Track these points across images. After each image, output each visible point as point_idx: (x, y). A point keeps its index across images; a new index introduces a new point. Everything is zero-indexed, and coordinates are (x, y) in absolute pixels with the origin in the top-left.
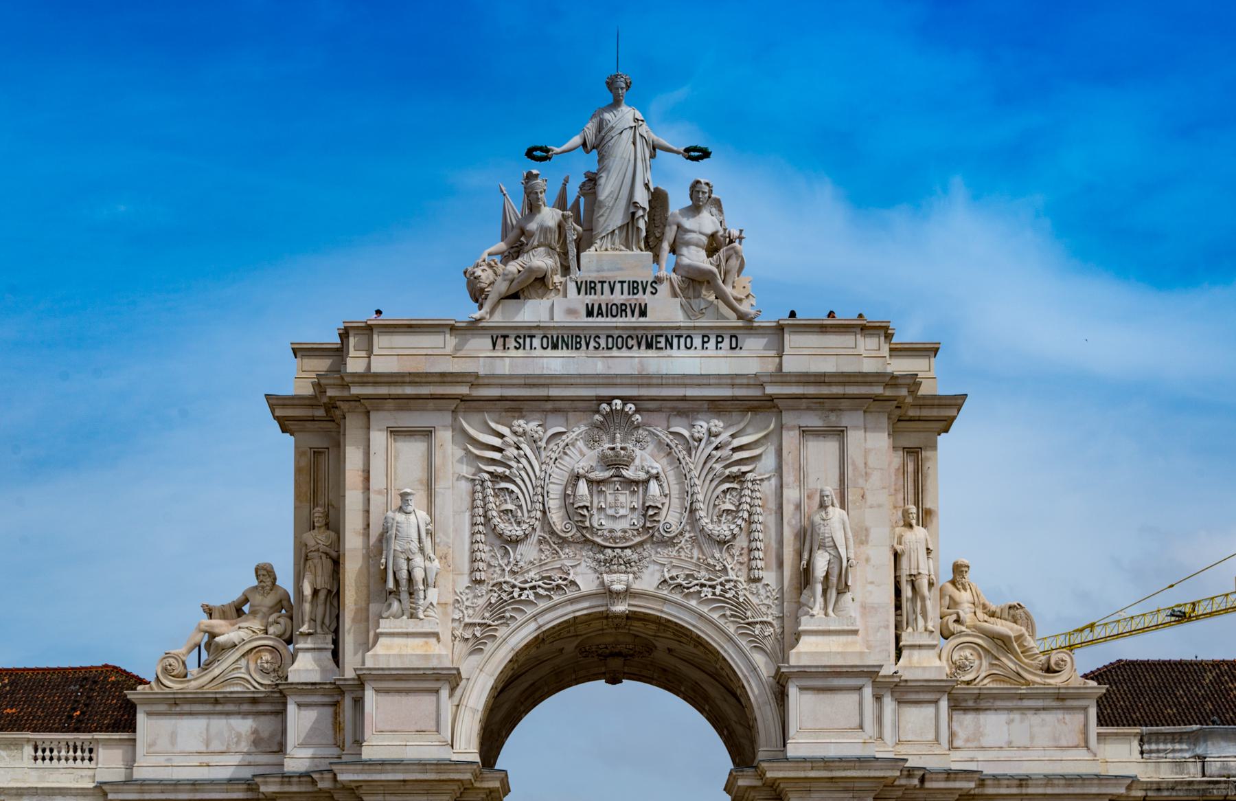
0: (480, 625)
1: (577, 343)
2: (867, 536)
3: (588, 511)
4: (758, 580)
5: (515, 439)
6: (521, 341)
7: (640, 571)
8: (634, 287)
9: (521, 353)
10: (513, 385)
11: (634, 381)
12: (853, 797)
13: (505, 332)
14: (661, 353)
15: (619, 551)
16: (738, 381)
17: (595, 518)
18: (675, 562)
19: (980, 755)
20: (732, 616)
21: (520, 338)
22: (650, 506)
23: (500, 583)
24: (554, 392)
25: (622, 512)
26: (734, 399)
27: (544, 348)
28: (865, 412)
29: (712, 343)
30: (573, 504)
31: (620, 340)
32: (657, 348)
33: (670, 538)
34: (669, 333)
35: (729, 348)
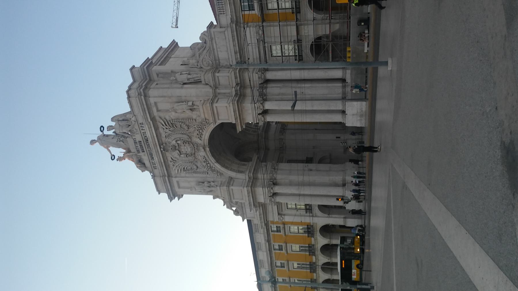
0: (217, 173)
4: (195, 120)
7: (199, 143)
8: (135, 143)
9: (156, 164)
10: (163, 169)
11: (156, 147)
12: (244, 108)
13: (153, 168)
14: (148, 138)
16: (150, 127)
18: (195, 137)
19: (231, 59)
20: (205, 126)
22: (183, 144)
24: (162, 161)
25: (186, 148)
26: (154, 126)
34: (143, 137)
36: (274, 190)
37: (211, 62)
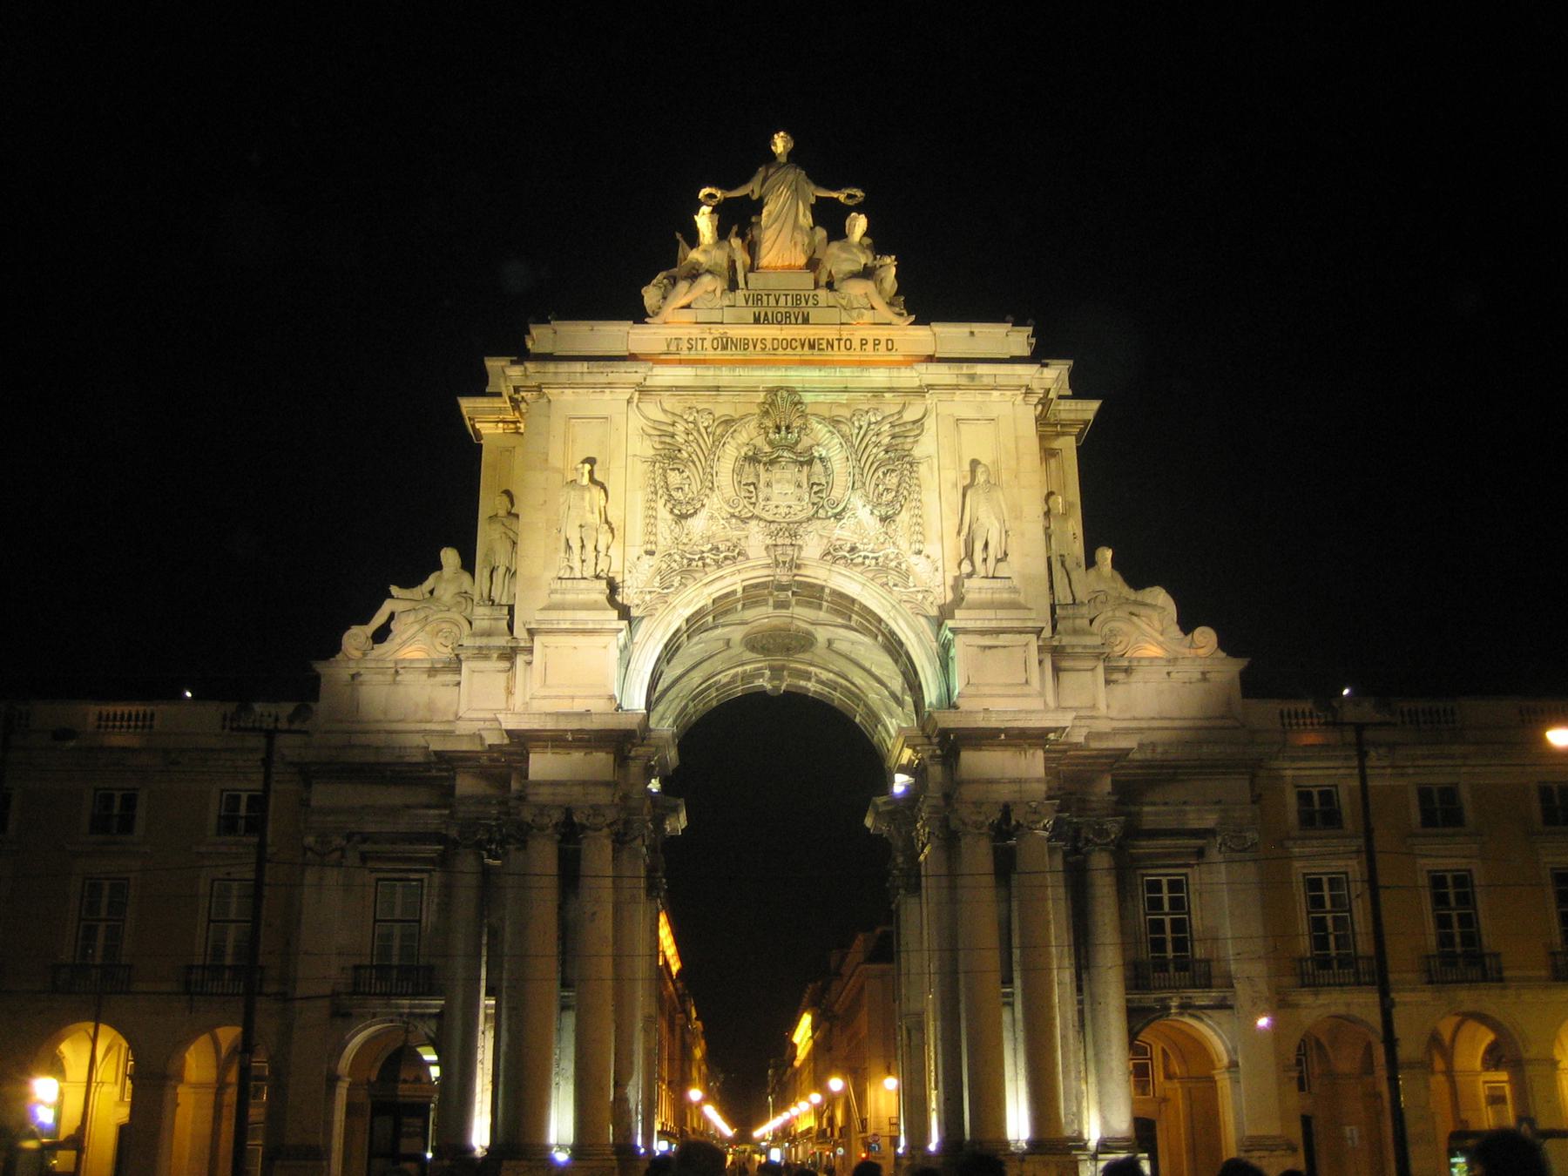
0: (650, 592)
1: (745, 344)
2: (1021, 512)
3: (756, 488)
4: (919, 552)
8: (797, 299)
15: (785, 525)
20: (895, 585)
21: (692, 340)
22: (813, 484)
23: (670, 555)
27: (715, 349)
28: (1013, 404)
29: (870, 346)
30: (740, 482)
31: (784, 342)
32: (819, 349)
33: (835, 516)
36: (606, 831)
37: (1118, 650)
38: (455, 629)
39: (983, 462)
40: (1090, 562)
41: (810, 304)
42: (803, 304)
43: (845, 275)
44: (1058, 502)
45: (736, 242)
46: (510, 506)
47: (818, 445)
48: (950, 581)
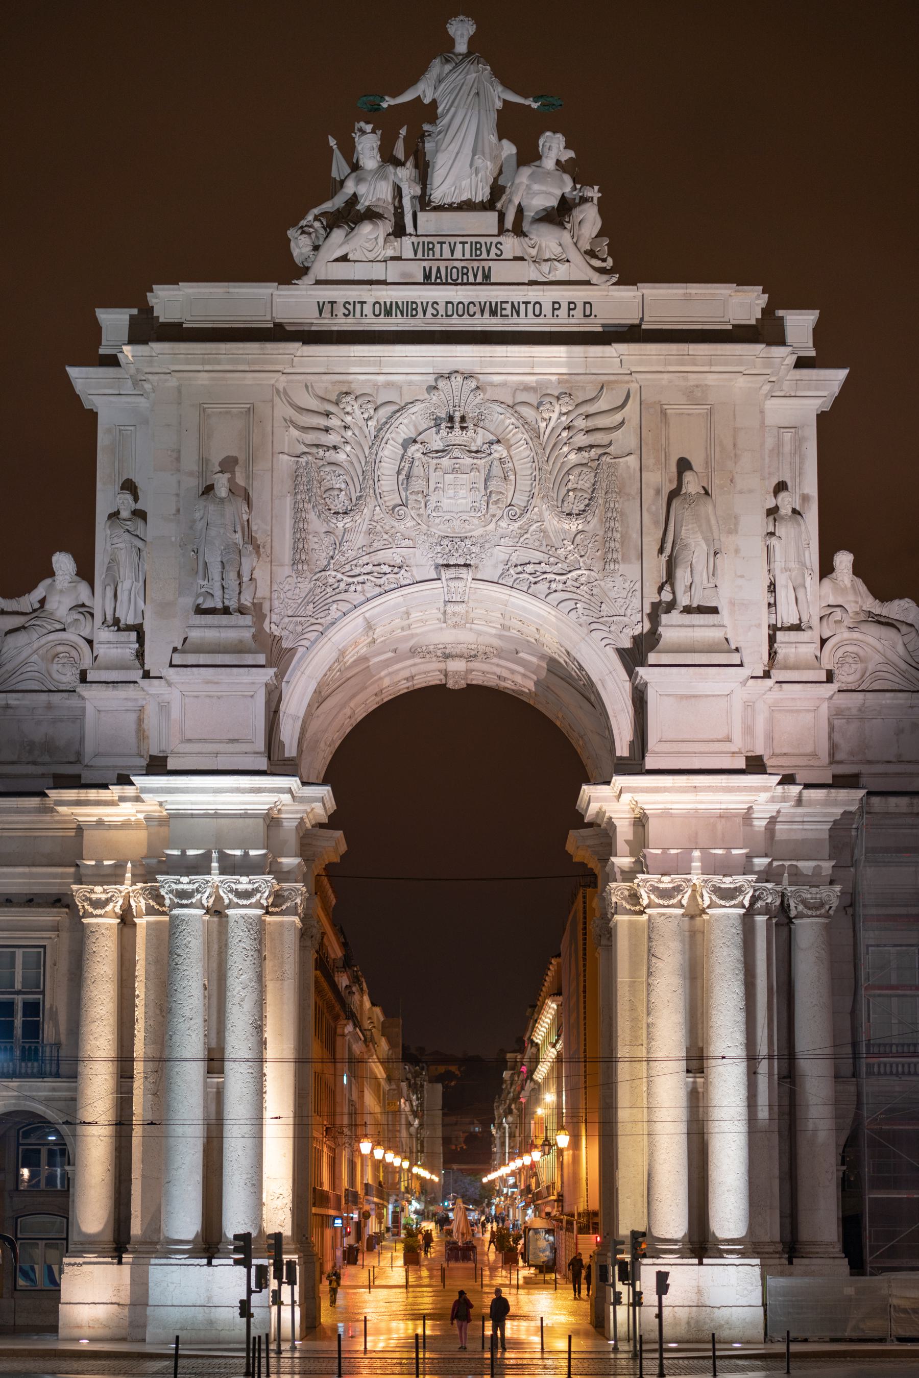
1: (413, 309)
2: (736, 524)
5: (342, 415)
6: (351, 307)
17: (433, 499)
29: (563, 312)
31: (461, 306)
32: (502, 316)
35: (582, 316)
38: (74, 653)
39: (695, 468)
40: (826, 569)
41: (492, 255)
42: (484, 256)
43: (537, 213)
44: (786, 502)
45: (405, 174)
46: (131, 502)
47: (498, 441)
48: (647, 609)
